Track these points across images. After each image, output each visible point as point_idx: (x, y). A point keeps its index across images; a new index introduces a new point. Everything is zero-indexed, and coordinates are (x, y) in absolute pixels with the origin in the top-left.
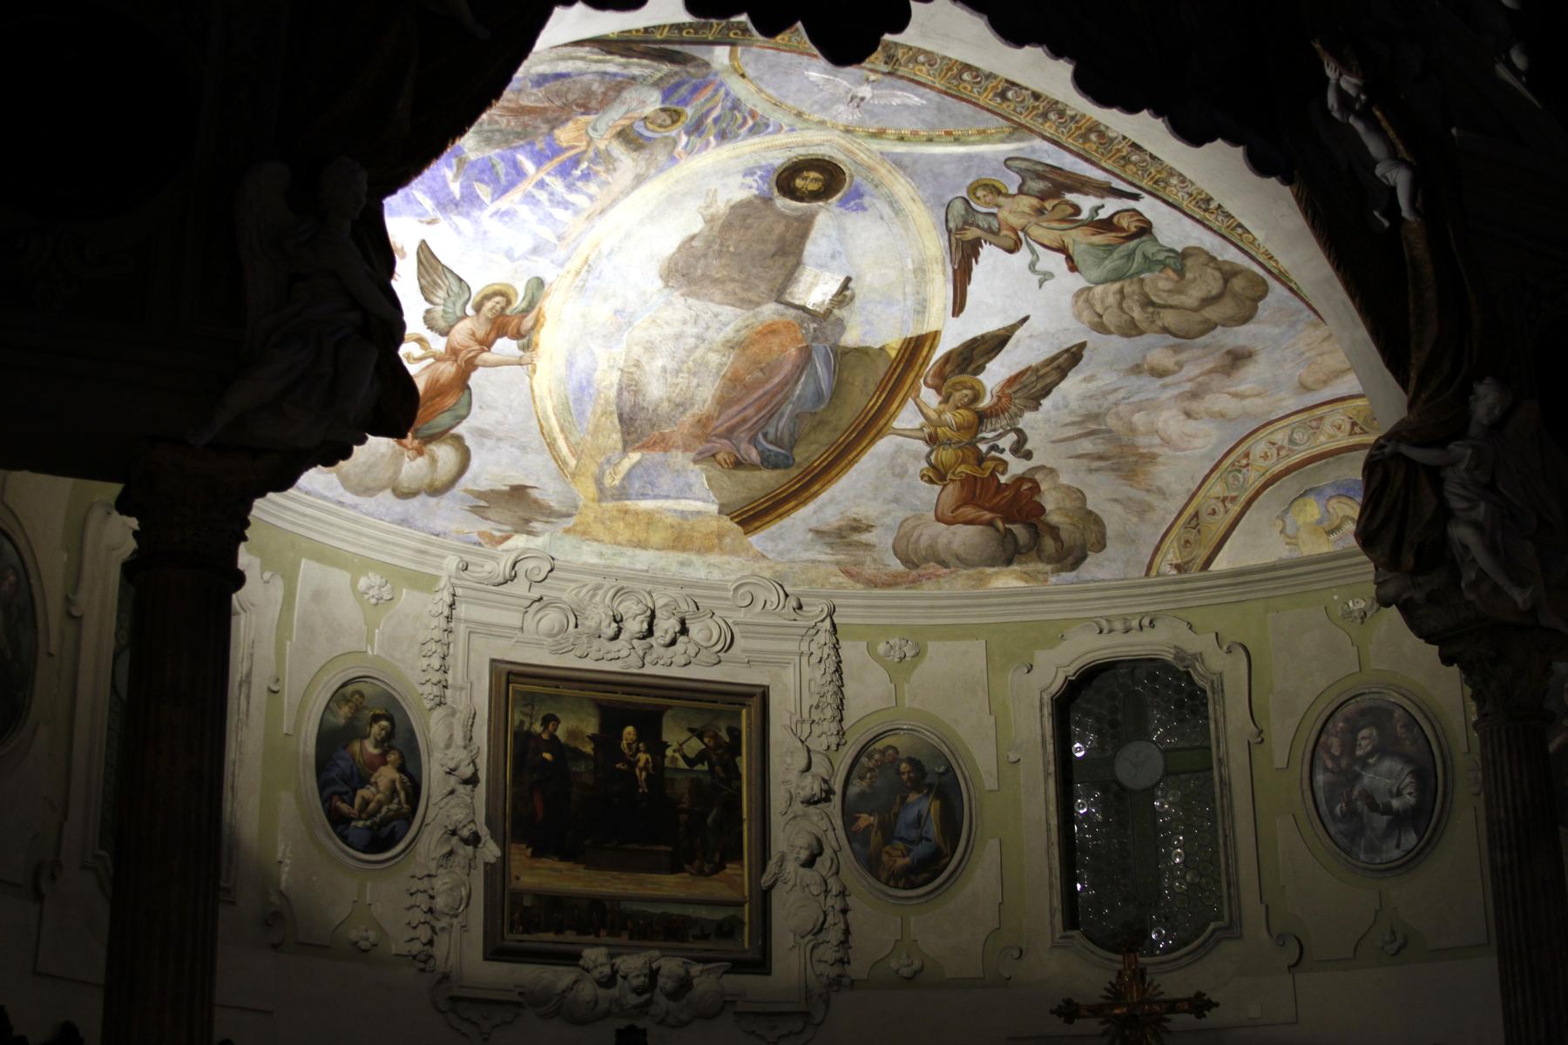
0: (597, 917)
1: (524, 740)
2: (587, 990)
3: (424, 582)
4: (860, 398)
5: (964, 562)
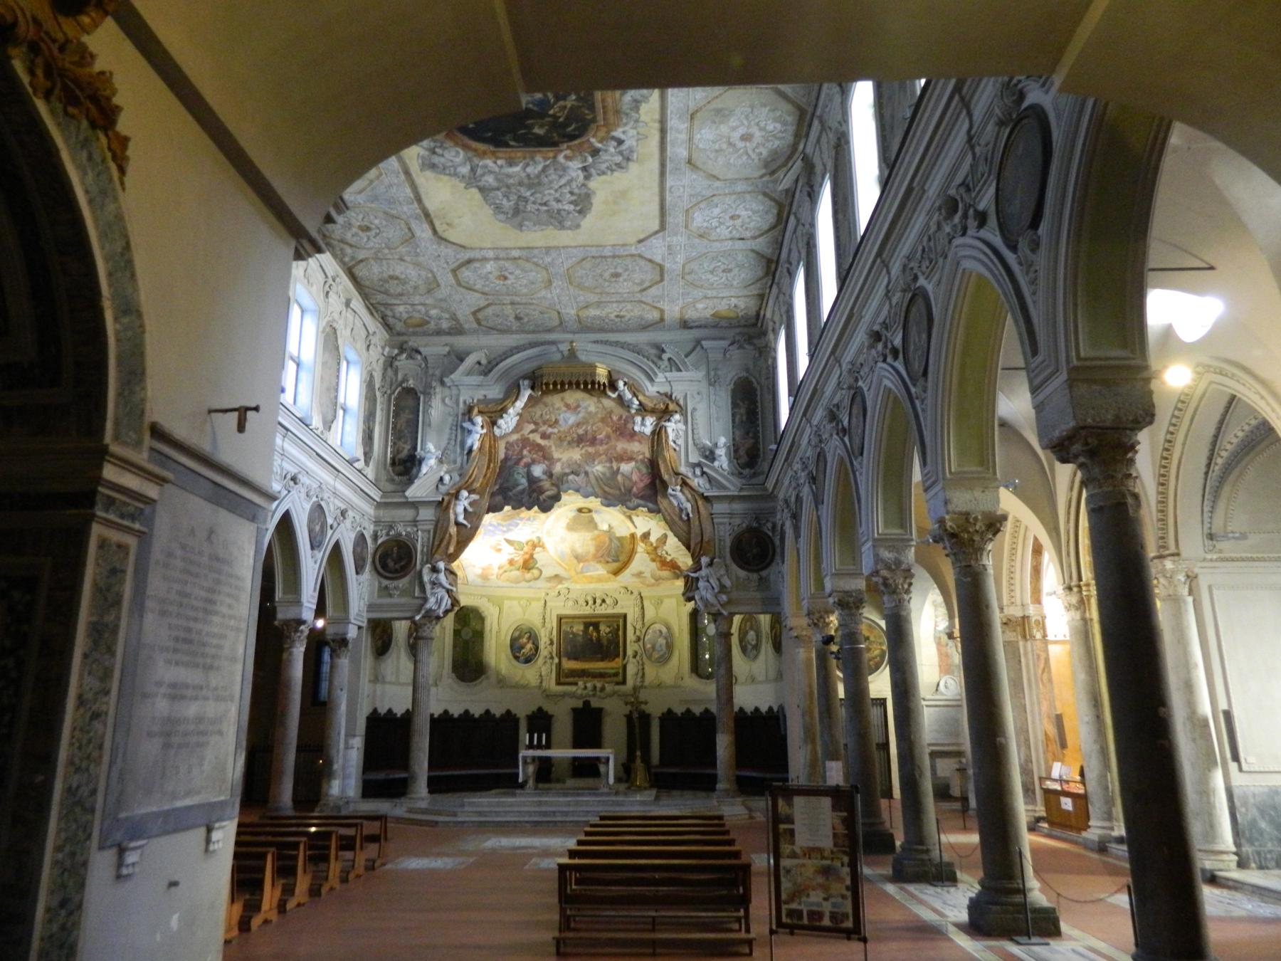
0: (583, 674)
1: (567, 633)
2: (579, 692)
3: (539, 600)
4: (628, 547)
5: (667, 579)
